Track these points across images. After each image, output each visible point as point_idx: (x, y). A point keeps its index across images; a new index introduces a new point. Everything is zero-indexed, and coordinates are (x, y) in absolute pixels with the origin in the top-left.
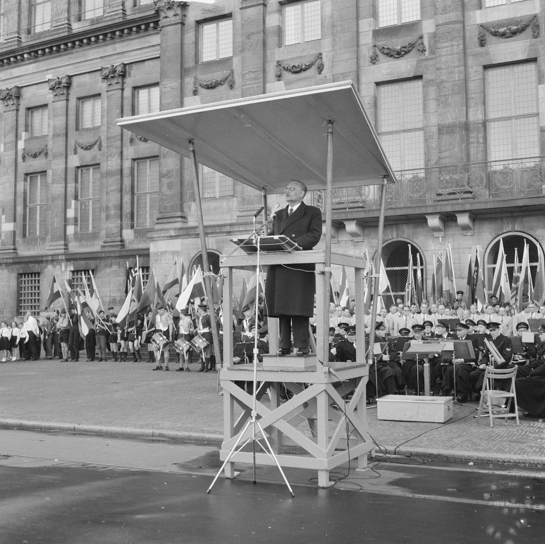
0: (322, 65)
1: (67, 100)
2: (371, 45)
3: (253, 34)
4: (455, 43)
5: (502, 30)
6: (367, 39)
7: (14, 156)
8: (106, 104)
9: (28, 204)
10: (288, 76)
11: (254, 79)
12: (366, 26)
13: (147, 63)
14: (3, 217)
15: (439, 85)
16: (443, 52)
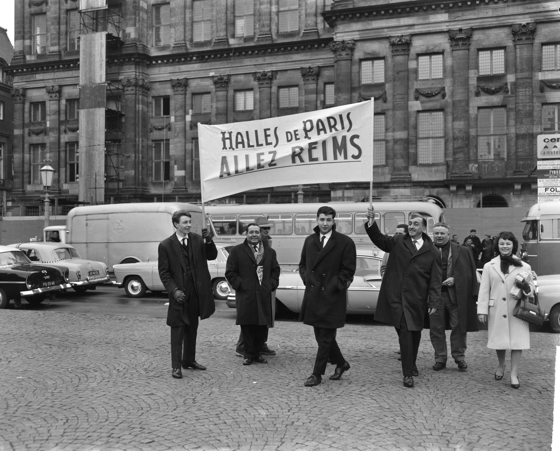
0: (445, 94)
1: (227, 91)
2: (476, 85)
3: (400, 71)
4: (527, 90)
5: (554, 85)
6: (473, 82)
7: (183, 126)
8: (258, 96)
9: (194, 158)
10: (423, 98)
11: (402, 99)
12: (472, 74)
13: (288, 72)
14: (176, 166)
15: (517, 112)
16: (520, 94)
